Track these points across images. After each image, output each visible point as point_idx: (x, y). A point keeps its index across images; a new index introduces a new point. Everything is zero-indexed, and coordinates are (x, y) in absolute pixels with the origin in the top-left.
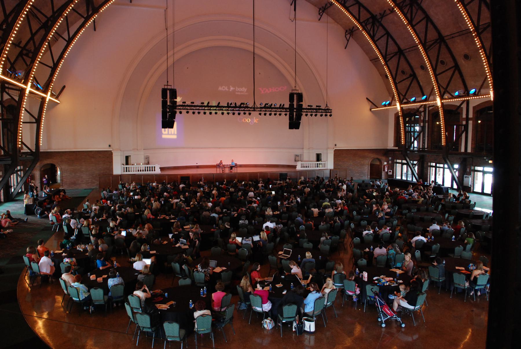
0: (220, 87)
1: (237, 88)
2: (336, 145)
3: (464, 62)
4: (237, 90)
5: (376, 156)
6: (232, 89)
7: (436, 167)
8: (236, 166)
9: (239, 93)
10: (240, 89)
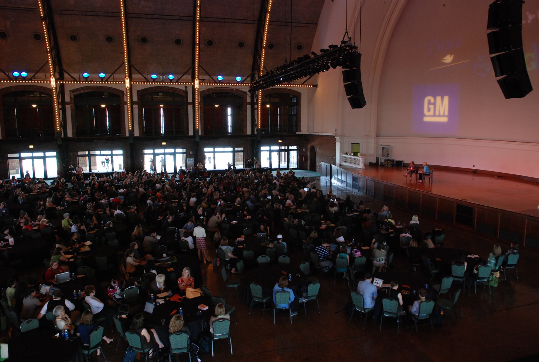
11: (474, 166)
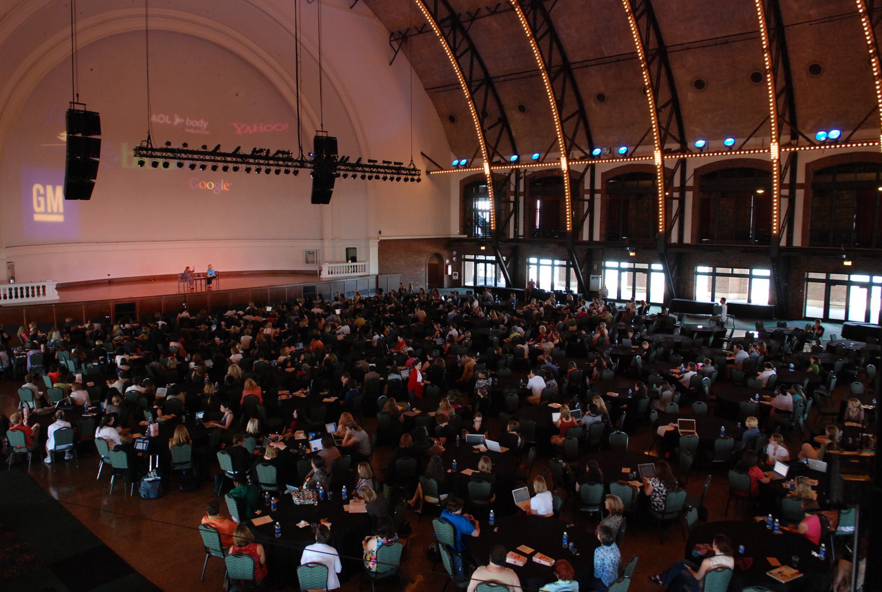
1: (188, 120)
2: (380, 232)
3: (594, 105)
4: (187, 124)
5: (436, 250)
6: (178, 120)
7: (538, 265)
8: (219, 275)
9: (192, 131)
10: (194, 123)
11: (109, 275)
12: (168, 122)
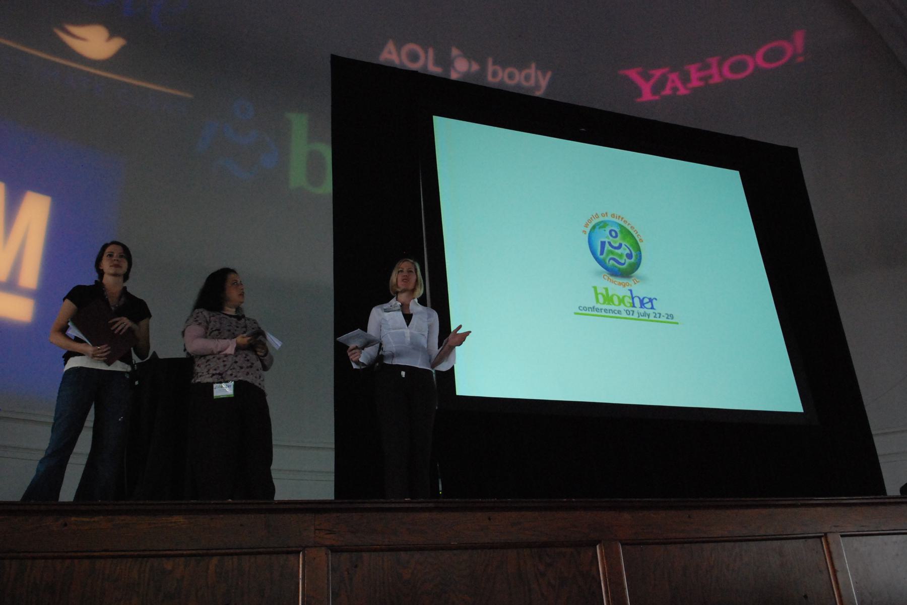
0: (391, 46)
1: (490, 68)
10: (511, 76)
12: (434, 69)
